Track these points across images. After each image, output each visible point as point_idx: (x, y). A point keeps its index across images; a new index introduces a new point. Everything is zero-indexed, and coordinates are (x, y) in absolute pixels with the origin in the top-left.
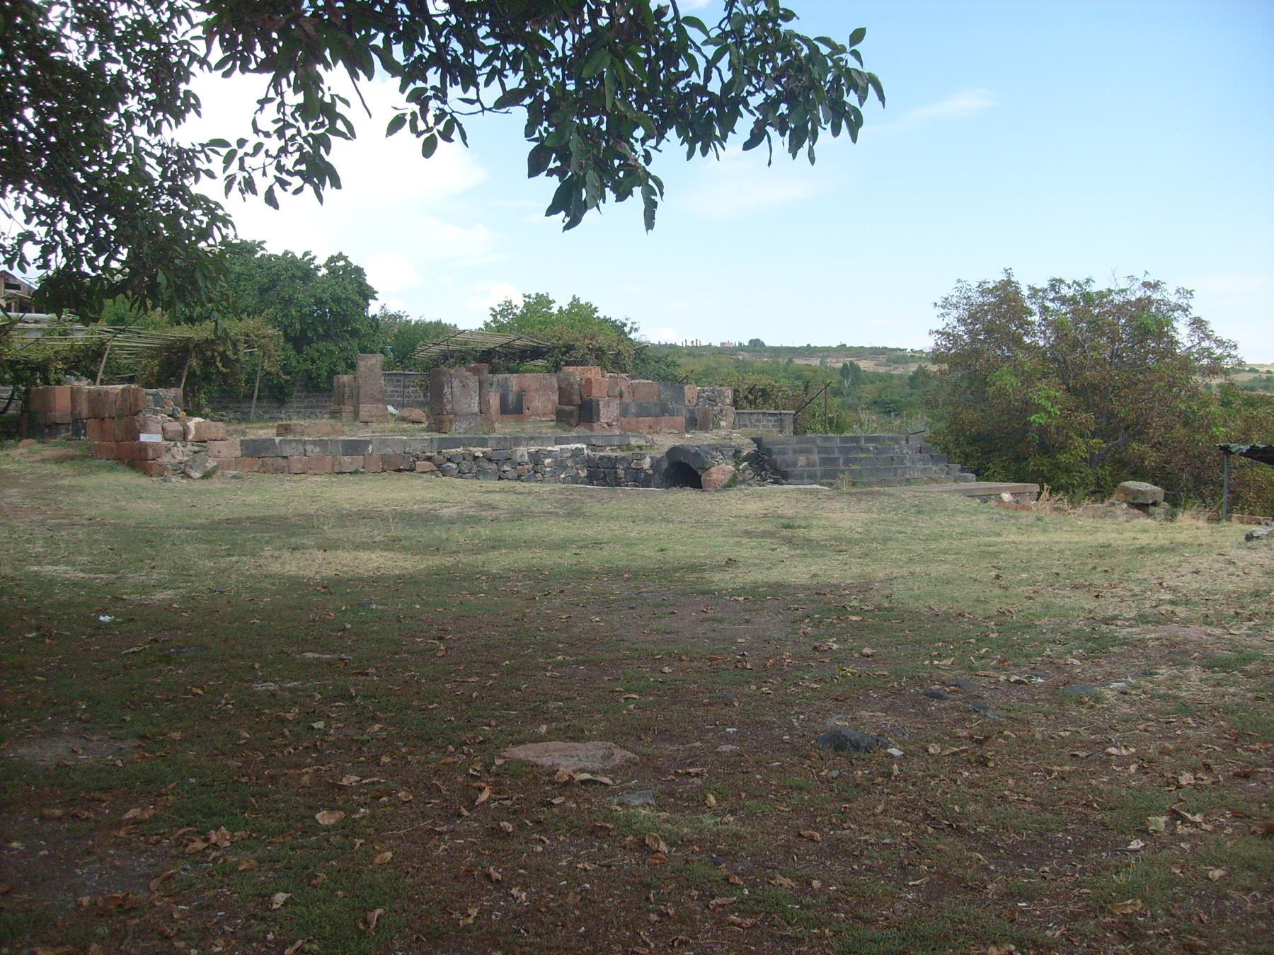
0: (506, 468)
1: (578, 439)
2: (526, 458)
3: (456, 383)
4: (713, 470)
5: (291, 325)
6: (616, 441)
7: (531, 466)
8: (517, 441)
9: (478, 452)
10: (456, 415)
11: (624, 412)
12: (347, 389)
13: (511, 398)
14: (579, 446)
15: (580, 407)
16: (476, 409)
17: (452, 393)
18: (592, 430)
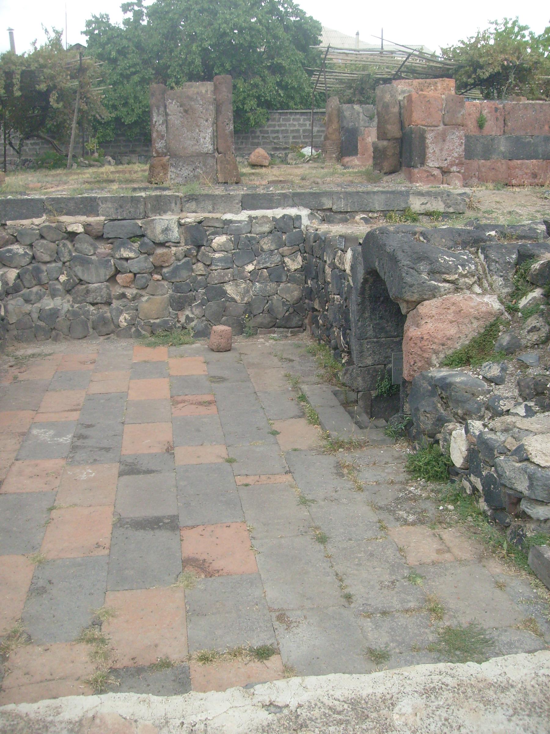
0: (126, 253)
1: (296, 199)
2: (175, 234)
3: (173, 107)
4: (428, 307)
5: (193, 62)
6: (378, 204)
7: (183, 248)
8: (160, 205)
9: (75, 224)
10: (174, 155)
11: (476, 148)
14: (292, 211)
16: (207, 146)
17: (166, 122)
18: (410, 179)
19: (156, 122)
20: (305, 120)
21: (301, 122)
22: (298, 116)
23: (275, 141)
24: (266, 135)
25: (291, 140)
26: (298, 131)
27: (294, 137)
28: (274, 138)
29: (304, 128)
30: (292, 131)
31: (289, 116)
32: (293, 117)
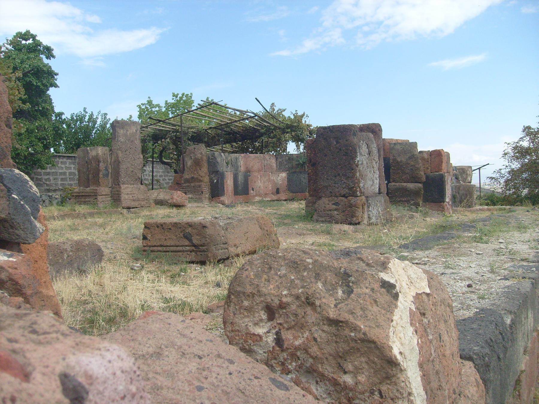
12: (102, 166)
13: (240, 178)
15: (424, 183)
19: (358, 161)
20: (70, 163)
21: (67, 165)
22: (65, 160)
23: (47, 183)
24: (39, 177)
25: (60, 182)
26: (65, 173)
27: (62, 179)
28: (46, 180)
29: (70, 171)
30: (61, 174)
31: (58, 159)
32: (61, 160)
